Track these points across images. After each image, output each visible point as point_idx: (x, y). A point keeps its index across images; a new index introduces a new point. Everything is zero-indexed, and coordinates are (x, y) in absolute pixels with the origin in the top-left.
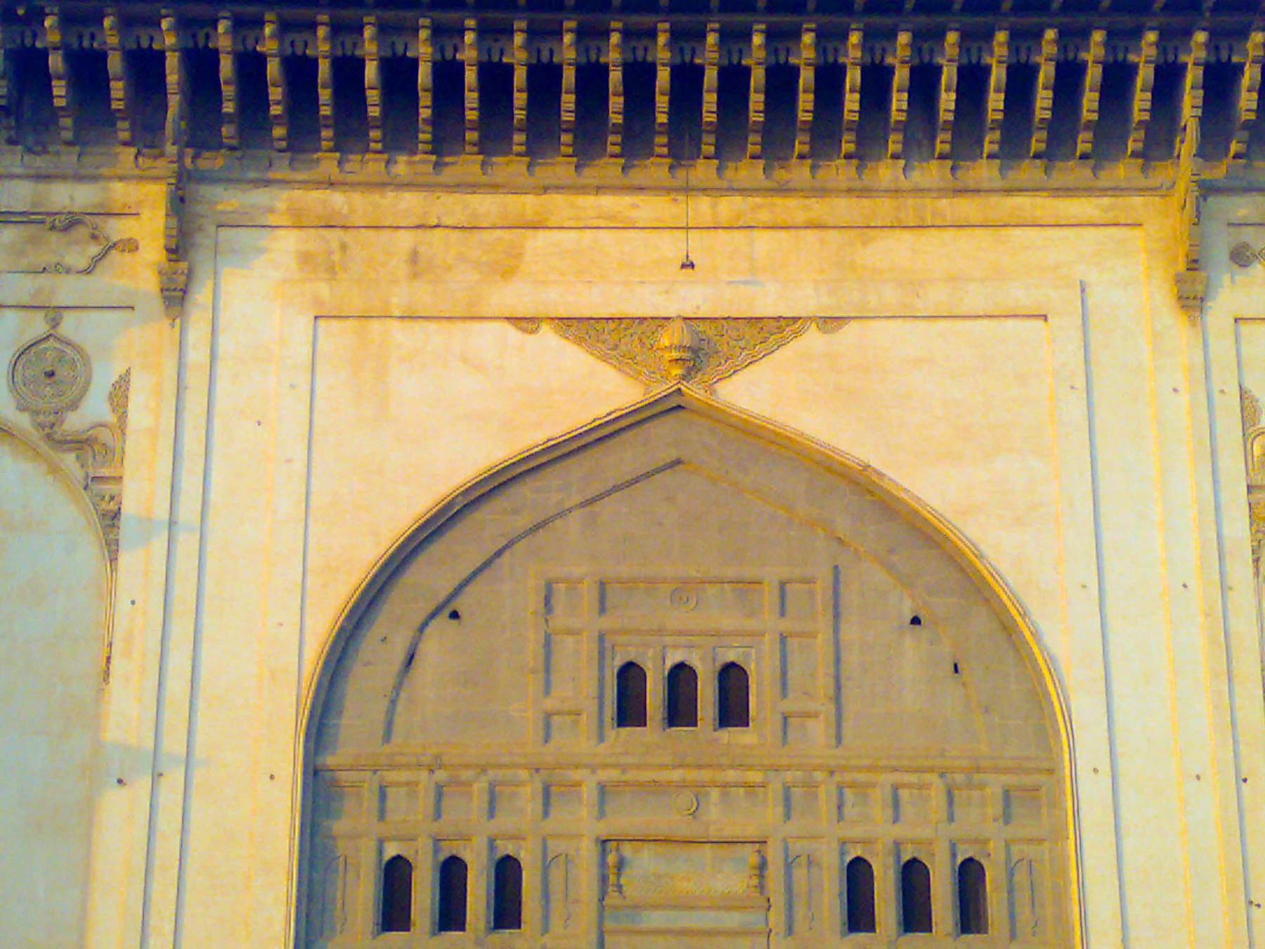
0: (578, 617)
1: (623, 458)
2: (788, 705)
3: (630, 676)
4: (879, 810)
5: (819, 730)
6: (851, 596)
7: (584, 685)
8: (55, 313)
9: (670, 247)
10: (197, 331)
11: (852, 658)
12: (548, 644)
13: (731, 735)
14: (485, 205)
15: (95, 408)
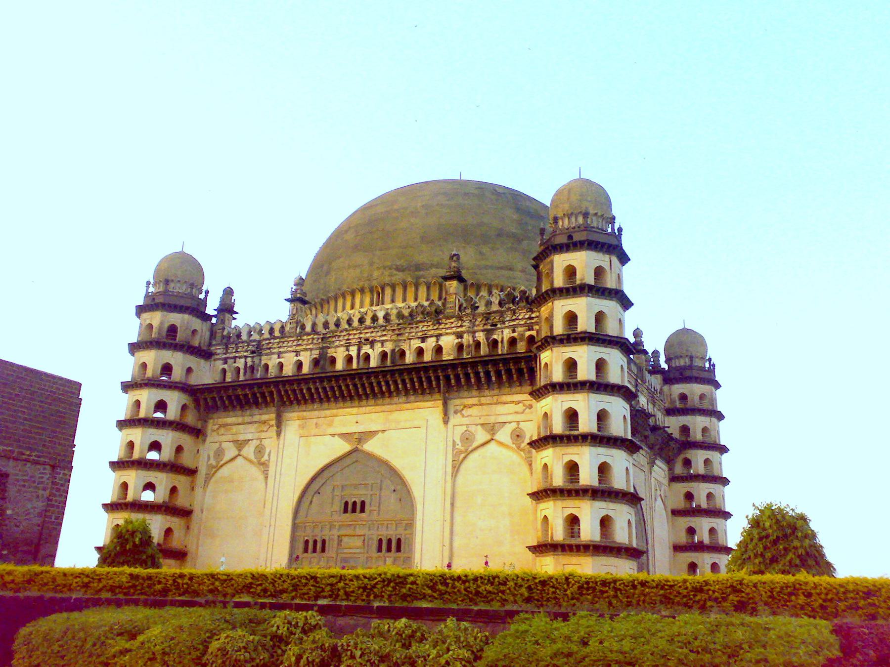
0: (337, 492)
1: (348, 461)
2: (373, 508)
3: (346, 503)
4: (384, 529)
5: (375, 513)
6: (384, 487)
7: (338, 506)
8: (261, 439)
9: (354, 419)
10: (281, 441)
11: (382, 499)
12: (333, 499)
13: (363, 515)
14: (328, 412)
15: (266, 457)
